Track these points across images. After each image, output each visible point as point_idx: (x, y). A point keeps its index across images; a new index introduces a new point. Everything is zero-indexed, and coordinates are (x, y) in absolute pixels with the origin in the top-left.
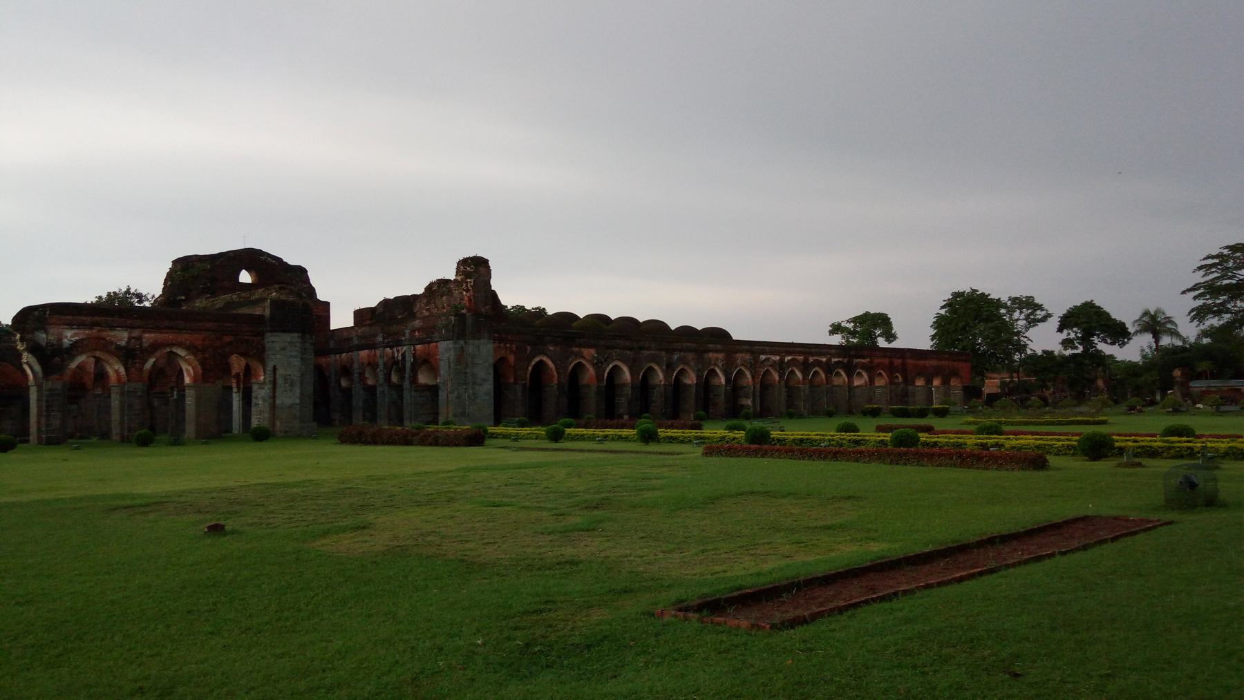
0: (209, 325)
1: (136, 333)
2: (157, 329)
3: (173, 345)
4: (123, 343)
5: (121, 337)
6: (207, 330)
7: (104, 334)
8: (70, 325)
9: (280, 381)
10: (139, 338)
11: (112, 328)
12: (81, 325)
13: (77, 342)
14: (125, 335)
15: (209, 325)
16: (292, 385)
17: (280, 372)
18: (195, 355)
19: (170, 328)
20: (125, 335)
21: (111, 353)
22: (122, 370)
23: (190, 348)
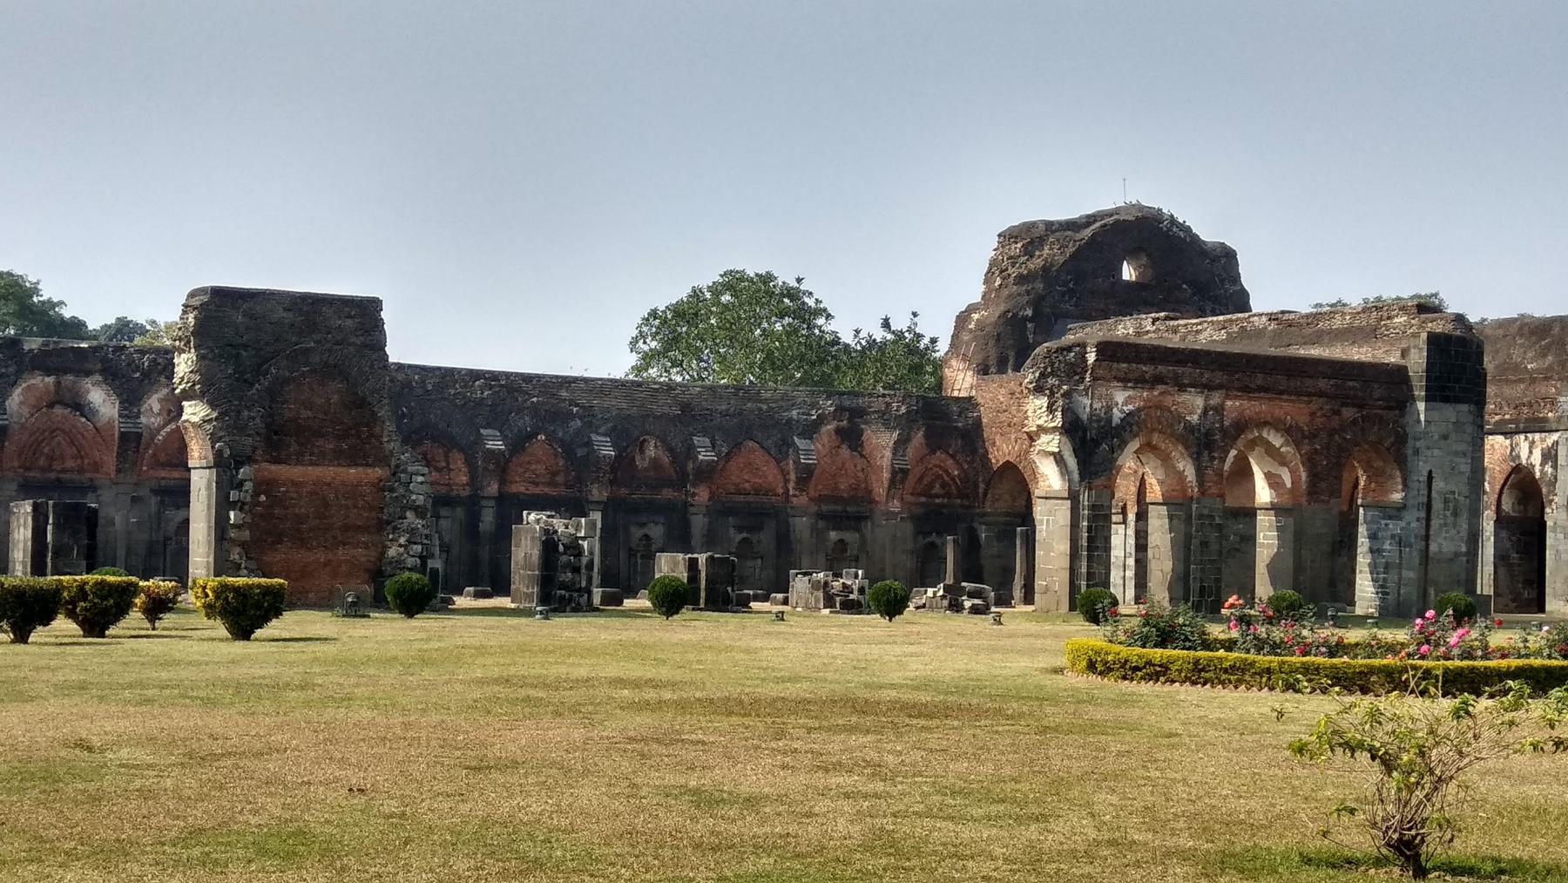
0: (1323, 384)
1: (1216, 399)
2: (1246, 390)
3: (1266, 423)
4: (1194, 419)
5: (1193, 405)
6: (1321, 394)
7: (1168, 401)
8: (1124, 380)
9: (1437, 505)
10: (1219, 410)
11: (1182, 388)
12: (1139, 382)
13: (1130, 414)
14: (1199, 402)
15: (1323, 384)
16: (1455, 514)
17: (1438, 484)
18: (1298, 445)
19: (1266, 390)
20: (1199, 402)
21: (1182, 439)
22: (1190, 473)
23: (1289, 431)
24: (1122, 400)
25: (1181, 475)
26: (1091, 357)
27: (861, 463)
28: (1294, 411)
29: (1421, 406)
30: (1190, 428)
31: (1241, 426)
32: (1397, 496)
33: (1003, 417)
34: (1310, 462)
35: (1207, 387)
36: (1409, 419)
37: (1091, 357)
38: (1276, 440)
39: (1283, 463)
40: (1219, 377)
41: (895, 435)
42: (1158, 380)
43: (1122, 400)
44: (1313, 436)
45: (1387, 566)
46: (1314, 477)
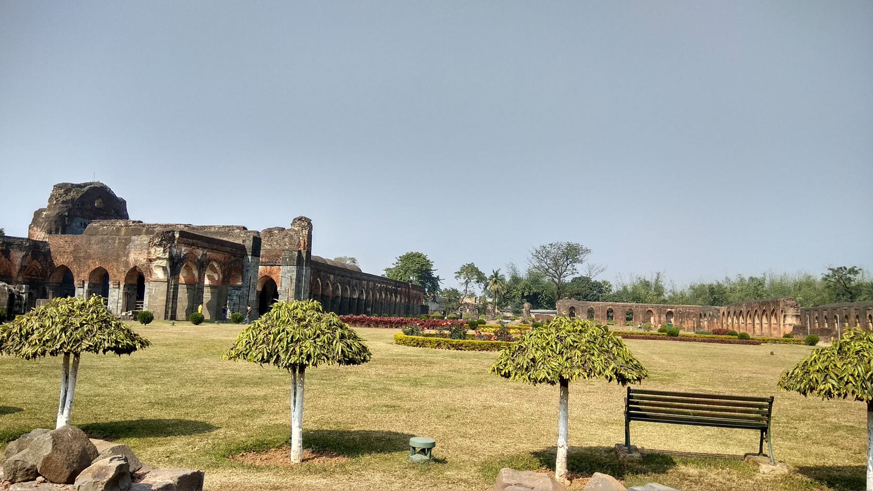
10: (206, 255)
14: (201, 252)
24: (184, 250)
25: (194, 275)
26: (177, 236)
27: (9, 263)
28: (220, 256)
29: (250, 257)
30: (199, 261)
31: (210, 260)
32: (240, 283)
33: (61, 249)
34: (223, 272)
35: (204, 248)
36: (246, 261)
37: (177, 236)
38: (216, 265)
39: (216, 272)
40: (207, 245)
41: (24, 253)
42: (193, 245)
43: (184, 250)
44: (224, 264)
45: (234, 305)
46: (224, 277)
